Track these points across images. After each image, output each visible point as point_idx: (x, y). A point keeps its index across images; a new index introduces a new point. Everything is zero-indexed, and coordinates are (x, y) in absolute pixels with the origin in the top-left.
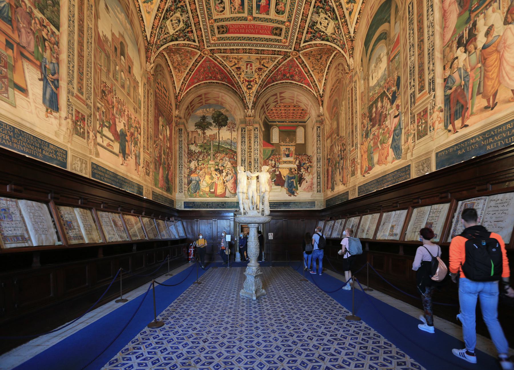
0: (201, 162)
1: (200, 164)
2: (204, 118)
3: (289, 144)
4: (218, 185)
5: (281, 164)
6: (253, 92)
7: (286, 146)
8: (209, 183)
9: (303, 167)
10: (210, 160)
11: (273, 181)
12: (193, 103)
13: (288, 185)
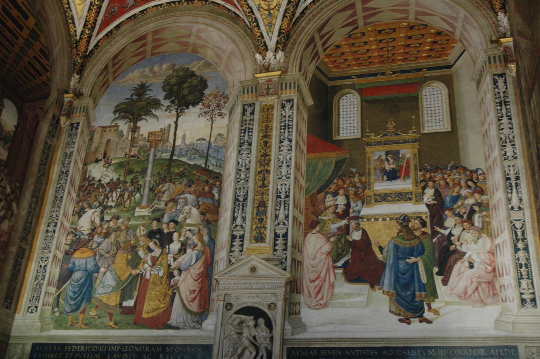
0: (113, 210)
1: (107, 218)
2: (141, 90)
3: (396, 138)
4: (150, 286)
5: (369, 204)
6: (279, 5)
7: (386, 143)
8: (123, 278)
9: (451, 209)
10: (138, 204)
11: (339, 264)
12: (119, 58)
13: (397, 280)
